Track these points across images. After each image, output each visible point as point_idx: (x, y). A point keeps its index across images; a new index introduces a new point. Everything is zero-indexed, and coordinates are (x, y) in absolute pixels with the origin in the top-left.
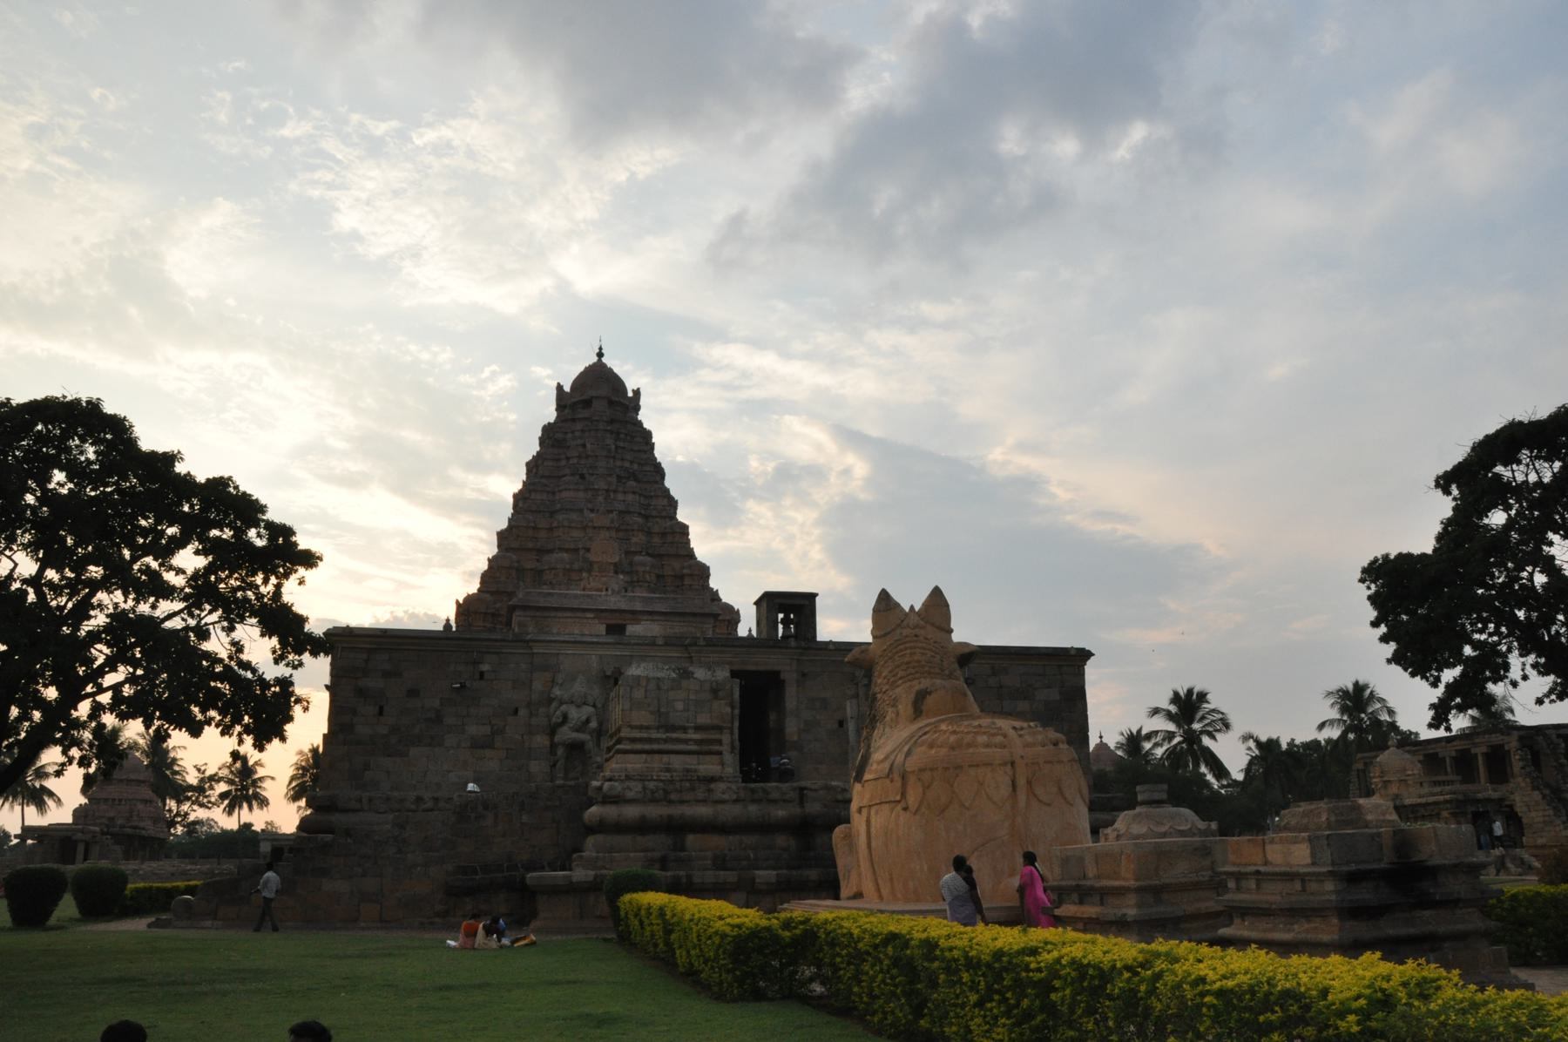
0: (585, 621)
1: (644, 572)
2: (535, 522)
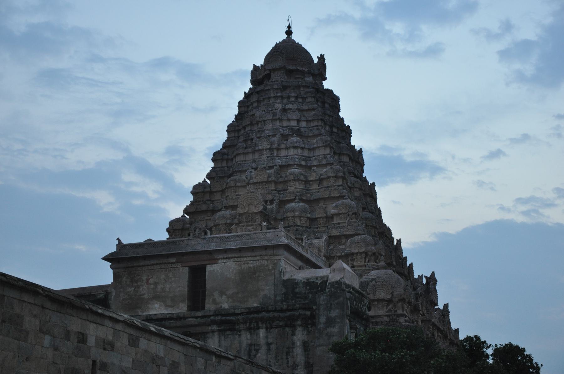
0: (169, 266)
1: (294, 217)
2: (210, 187)
